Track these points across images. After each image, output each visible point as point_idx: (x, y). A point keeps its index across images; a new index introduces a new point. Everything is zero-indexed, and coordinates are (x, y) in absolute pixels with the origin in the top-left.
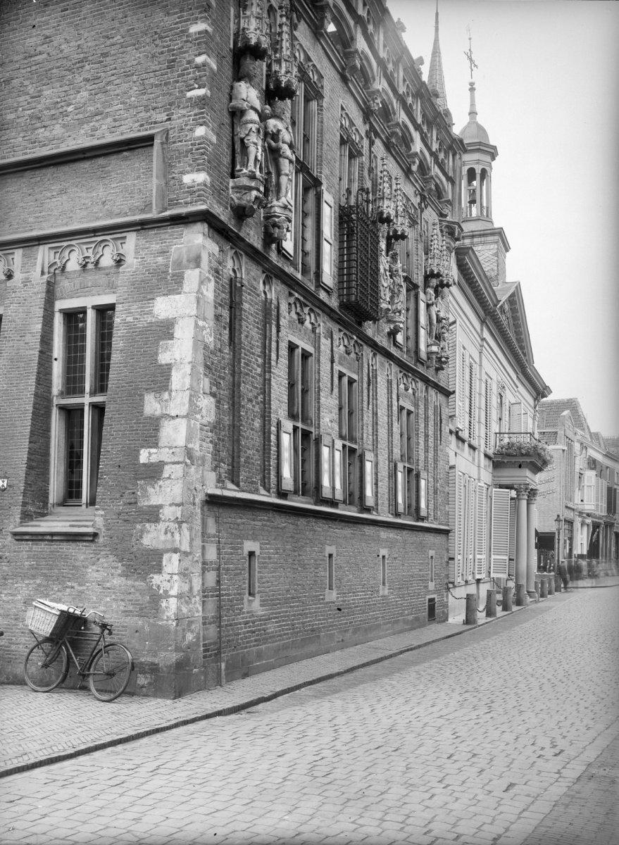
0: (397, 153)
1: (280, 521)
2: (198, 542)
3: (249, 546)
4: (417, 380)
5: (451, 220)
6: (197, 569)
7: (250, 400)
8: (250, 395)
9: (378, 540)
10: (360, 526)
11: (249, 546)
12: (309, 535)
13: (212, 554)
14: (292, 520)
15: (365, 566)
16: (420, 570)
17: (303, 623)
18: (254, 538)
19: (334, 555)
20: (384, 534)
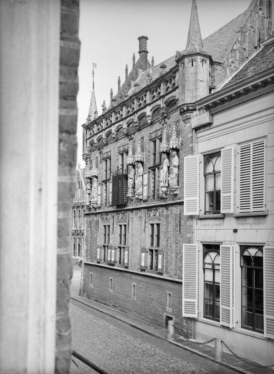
0: (143, 126)
1: (98, 269)
2: (83, 271)
3: (91, 273)
4: (159, 208)
6: (83, 275)
7: (93, 243)
8: (92, 242)
9: (131, 279)
10: (123, 273)
11: (91, 273)
12: (105, 273)
13: (85, 274)
14: (100, 268)
15: (125, 286)
16: (158, 298)
17: (103, 295)
18: (92, 272)
19: (112, 280)
20: (134, 277)
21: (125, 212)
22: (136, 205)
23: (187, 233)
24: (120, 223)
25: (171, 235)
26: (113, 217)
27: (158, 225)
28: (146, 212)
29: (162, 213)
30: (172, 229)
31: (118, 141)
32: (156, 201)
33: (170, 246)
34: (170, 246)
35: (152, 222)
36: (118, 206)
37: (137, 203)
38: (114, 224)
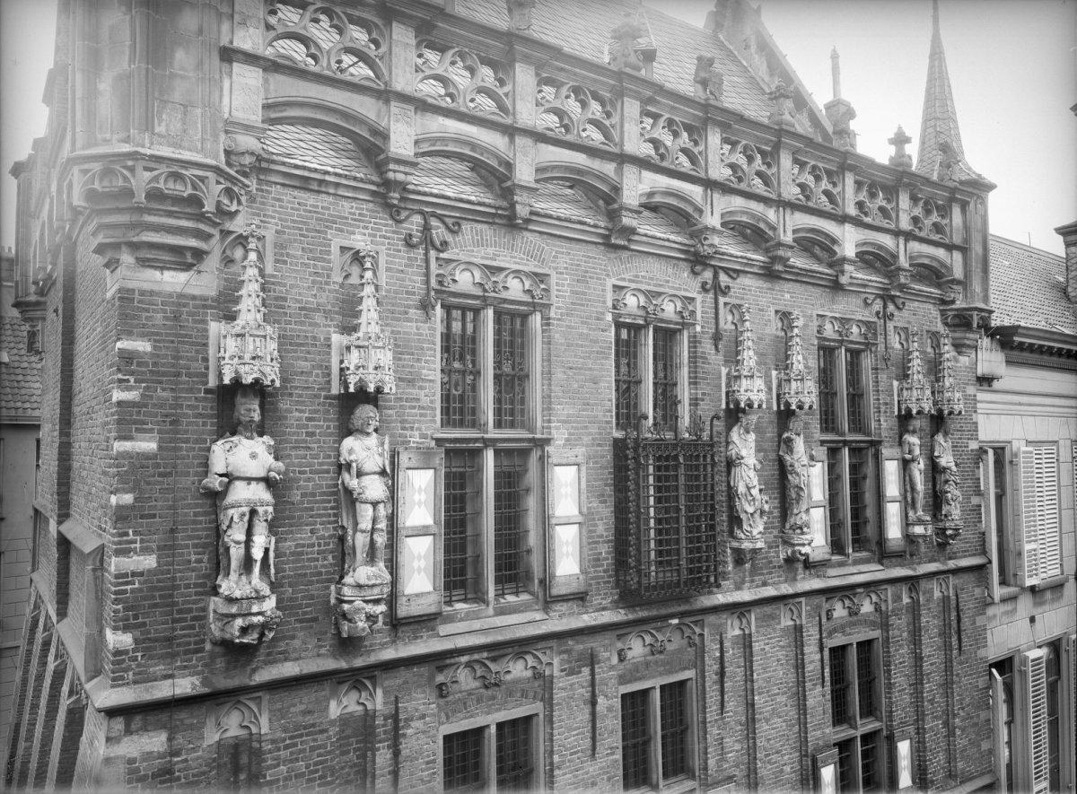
5: (964, 306)
21: (687, 620)
22: (765, 584)
23: (979, 648)
24: (640, 679)
25: (931, 664)
26: (592, 660)
27: (865, 646)
28: (819, 607)
29: (894, 601)
30: (932, 647)
31: (625, 254)
32: (856, 563)
33: (929, 701)
34: (929, 701)
35: (838, 640)
36: (627, 598)
37: (771, 573)
38: (601, 700)
